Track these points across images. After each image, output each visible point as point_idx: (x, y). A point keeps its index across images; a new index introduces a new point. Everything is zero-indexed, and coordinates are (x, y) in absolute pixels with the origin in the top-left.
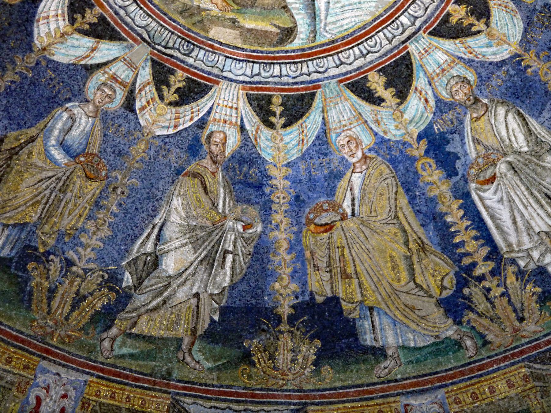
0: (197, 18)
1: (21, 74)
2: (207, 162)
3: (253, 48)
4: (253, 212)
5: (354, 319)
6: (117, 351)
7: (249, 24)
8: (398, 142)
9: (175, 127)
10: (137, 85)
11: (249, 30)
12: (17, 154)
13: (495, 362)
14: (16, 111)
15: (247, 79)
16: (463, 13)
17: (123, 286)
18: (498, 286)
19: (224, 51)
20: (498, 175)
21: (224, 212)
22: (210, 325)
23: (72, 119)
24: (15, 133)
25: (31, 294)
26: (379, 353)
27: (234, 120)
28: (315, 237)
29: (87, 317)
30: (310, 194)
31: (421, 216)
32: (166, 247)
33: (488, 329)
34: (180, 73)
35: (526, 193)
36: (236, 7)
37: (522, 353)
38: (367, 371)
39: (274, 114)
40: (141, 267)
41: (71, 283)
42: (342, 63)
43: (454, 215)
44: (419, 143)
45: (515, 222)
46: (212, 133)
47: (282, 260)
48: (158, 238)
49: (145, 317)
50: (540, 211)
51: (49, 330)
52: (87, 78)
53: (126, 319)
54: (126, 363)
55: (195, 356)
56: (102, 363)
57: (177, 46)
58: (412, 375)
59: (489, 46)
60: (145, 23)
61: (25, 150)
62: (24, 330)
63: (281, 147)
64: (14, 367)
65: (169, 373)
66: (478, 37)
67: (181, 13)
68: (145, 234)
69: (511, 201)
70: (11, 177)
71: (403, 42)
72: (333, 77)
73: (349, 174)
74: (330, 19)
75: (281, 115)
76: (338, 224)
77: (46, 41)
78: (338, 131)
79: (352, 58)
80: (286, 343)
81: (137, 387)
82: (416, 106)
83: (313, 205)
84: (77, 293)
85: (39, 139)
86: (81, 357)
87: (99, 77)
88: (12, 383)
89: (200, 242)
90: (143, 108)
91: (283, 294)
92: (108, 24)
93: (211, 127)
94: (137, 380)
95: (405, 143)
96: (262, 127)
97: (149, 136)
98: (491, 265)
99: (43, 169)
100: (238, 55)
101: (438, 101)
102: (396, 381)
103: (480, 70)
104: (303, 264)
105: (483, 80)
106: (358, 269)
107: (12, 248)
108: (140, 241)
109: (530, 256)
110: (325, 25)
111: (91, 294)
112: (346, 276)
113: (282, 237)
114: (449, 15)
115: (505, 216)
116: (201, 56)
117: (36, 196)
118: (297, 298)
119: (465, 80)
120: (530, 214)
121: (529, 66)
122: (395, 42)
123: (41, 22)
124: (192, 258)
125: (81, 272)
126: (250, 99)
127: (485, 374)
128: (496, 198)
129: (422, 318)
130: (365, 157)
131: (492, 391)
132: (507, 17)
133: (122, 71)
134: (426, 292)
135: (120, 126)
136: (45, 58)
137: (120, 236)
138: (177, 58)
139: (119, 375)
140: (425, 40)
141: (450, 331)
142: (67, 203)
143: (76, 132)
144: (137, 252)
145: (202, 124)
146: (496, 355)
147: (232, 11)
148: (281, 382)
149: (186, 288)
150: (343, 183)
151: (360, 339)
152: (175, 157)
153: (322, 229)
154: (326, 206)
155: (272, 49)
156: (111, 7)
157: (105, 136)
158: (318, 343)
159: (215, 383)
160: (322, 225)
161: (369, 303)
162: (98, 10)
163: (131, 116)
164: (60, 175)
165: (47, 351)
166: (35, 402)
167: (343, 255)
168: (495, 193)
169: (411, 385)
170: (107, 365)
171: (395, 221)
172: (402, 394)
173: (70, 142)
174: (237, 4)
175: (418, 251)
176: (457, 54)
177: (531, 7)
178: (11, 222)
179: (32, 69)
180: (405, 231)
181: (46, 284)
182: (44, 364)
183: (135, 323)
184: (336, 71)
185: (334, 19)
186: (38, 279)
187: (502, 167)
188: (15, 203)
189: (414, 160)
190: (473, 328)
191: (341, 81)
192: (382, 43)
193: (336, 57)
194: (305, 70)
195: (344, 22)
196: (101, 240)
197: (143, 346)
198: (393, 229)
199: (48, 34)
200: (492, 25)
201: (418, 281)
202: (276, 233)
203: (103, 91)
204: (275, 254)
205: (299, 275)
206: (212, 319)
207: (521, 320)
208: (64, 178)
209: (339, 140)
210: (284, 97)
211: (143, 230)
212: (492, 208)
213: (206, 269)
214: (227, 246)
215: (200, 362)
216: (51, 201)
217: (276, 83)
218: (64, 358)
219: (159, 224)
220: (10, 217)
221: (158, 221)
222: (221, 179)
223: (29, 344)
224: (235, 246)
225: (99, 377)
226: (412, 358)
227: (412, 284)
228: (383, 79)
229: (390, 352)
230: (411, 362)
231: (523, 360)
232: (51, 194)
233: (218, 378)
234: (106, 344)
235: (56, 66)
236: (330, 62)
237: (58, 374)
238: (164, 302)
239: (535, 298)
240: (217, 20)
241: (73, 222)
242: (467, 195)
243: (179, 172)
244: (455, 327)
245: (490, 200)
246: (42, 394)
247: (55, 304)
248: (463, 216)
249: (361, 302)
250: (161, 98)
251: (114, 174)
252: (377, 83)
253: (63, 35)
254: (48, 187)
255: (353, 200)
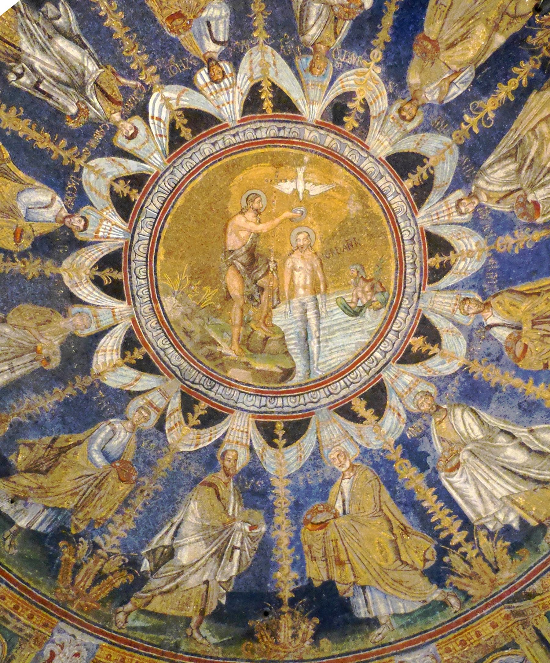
0: (219, 361)
1: (77, 390)
2: (221, 474)
3: (261, 385)
4: (258, 516)
5: (349, 598)
6: (130, 623)
7: (258, 366)
8: (378, 450)
9: (197, 445)
10: (168, 411)
11: (259, 371)
12: (65, 452)
13: (477, 611)
14: (69, 419)
15: (256, 409)
16: (421, 343)
17: (142, 570)
18: (473, 548)
19: (238, 387)
20: (462, 461)
21: (233, 515)
22: (217, 607)
23: (114, 431)
24: (66, 436)
25: (59, 566)
26: (373, 623)
27: (244, 442)
28: (312, 534)
29: (107, 592)
30: (307, 499)
31: (402, 507)
32: (181, 542)
33: (469, 586)
34: (203, 405)
35: (486, 470)
36: (249, 353)
37: (501, 597)
38: (362, 639)
39: (277, 437)
40: (158, 557)
41: (96, 563)
42: (331, 394)
43: (429, 500)
44: (395, 448)
45: (480, 495)
46: (226, 451)
47: (284, 554)
48: (176, 534)
49: (159, 598)
50: (499, 481)
51: (70, 598)
52: (129, 401)
53: (141, 598)
54: (138, 634)
55: (202, 633)
56: (117, 633)
57: (202, 382)
58: (405, 636)
59: (443, 363)
60: (178, 363)
61: (72, 450)
62: (48, 594)
63: (283, 464)
64: (34, 623)
65: (177, 646)
66: (434, 358)
67: (207, 357)
68: (164, 530)
69: (475, 479)
70: (57, 469)
71: (378, 372)
72: (325, 405)
73: (339, 481)
74: (321, 360)
75: (283, 437)
76: (332, 522)
77: (102, 369)
78: (330, 447)
79: (339, 389)
80: (286, 622)
81: (146, 655)
82: (390, 421)
83: (310, 508)
84: (100, 571)
85: (84, 443)
86: (96, 624)
87: (139, 401)
88: (30, 636)
89: (211, 539)
90: (171, 429)
91: (285, 580)
92: (151, 360)
93: (225, 447)
94: (146, 649)
95: (383, 451)
96: (268, 447)
97: (175, 451)
98: (465, 533)
99: (84, 468)
100: (250, 390)
101: (408, 412)
102: (390, 643)
103: (439, 383)
104: (302, 558)
105: (441, 391)
106: (350, 556)
107: (49, 526)
108: (158, 536)
109: (497, 519)
110: (318, 365)
111: (112, 574)
112: (340, 563)
113: (283, 535)
114: (411, 346)
115: (472, 493)
116: (220, 391)
117: (76, 488)
118: (297, 583)
119: (428, 394)
120: (492, 486)
121: (474, 373)
122: (372, 373)
123: (100, 353)
124: (203, 551)
125: (105, 555)
126: (258, 425)
127: (470, 623)
128: (463, 479)
129: (410, 588)
130: (352, 466)
131: (478, 634)
132: (454, 338)
133: (157, 399)
134: (412, 566)
135: (151, 441)
136: (99, 381)
137: (142, 530)
138: (201, 392)
139: (130, 644)
140: (394, 368)
141: (435, 594)
142: (100, 498)
143: (115, 443)
144: (157, 544)
145: (218, 444)
146: (478, 605)
147: (246, 356)
148: (282, 654)
149: (197, 576)
150: (334, 490)
151: (355, 614)
152: (194, 469)
153: (318, 527)
154: (321, 508)
155: (276, 386)
156: (154, 348)
157: (138, 447)
158: (317, 620)
159: (220, 656)
160: (317, 524)
161: (361, 582)
162: (144, 350)
163: (161, 435)
164: (97, 475)
165: (66, 615)
166: (49, 655)
167: (337, 546)
168: (461, 476)
169: (404, 645)
170: (122, 634)
171: (380, 514)
172: (396, 654)
173: (108, 450)
174: (250, 351)
175: (401, 535)
176: (420, 374)
177: (470, 328)
178: (51, 505)
179: (88, 388)
180: (389, 521)
181: (74, 561)
182: (62, 625)
183: (149, 602)
184: (327, 400)
185: (323, 360)
186: (67, 555)
187: (464, 455)
188: (57, 490)
189: (392, 462)
190: (456, 588)
191: (330, 408)
192: (361, 375)
193: (326, 389)
194: (302, 401)
195: (331, 362)
196: (126, 531)
197: (154, 621)
198: (378, 521)
199: (104, 363)
200: (443, 347)
201: (403, 558)
202: (278, 532)
203: (141, 413)
204: (278, 549)
205: (299, 565)
206: (219, 601)
207: (496, 571)
208: (100, 478)
209: (331, 456)
210: (285, 423)
211: (162, 527)
212: (460, 489)
213: (216, 561)
214: (235, 543)
215: (207, 638)
216: (87, 494)
217: (279, 413)
218: (81, 623)
219: (177, 523)
220: (51, 502)
221: (176, 520)
222: (232, 490)
223: (52, 607)
224: (242, 543)
225: (111, 643)
226: (404, 623)
227: (399, 563)
228: (364, 403)
229: (382, 621)
230: (402, 626)
231: (503, 604)
232: (88, 488)
233: (223, 652)
234: (121, 616)
235: (106, 389)
236: (321, 394)
237: (74, 636)
238: (177, 587)
239: (506, 550)
240: (234, 363)
241: (104, 514)
242: (439, 482)
243: (197, 481)
244: (439, 591)
245: (457, 483)
246: (57, 650)
247: (79, 578)
248: (438, 500)
249: (354, 583)
250: (187, 422)
251: (142, 479)
252: (359, 406)
253: (115, 366)
254: (86, 483)
255: (344, 501)
